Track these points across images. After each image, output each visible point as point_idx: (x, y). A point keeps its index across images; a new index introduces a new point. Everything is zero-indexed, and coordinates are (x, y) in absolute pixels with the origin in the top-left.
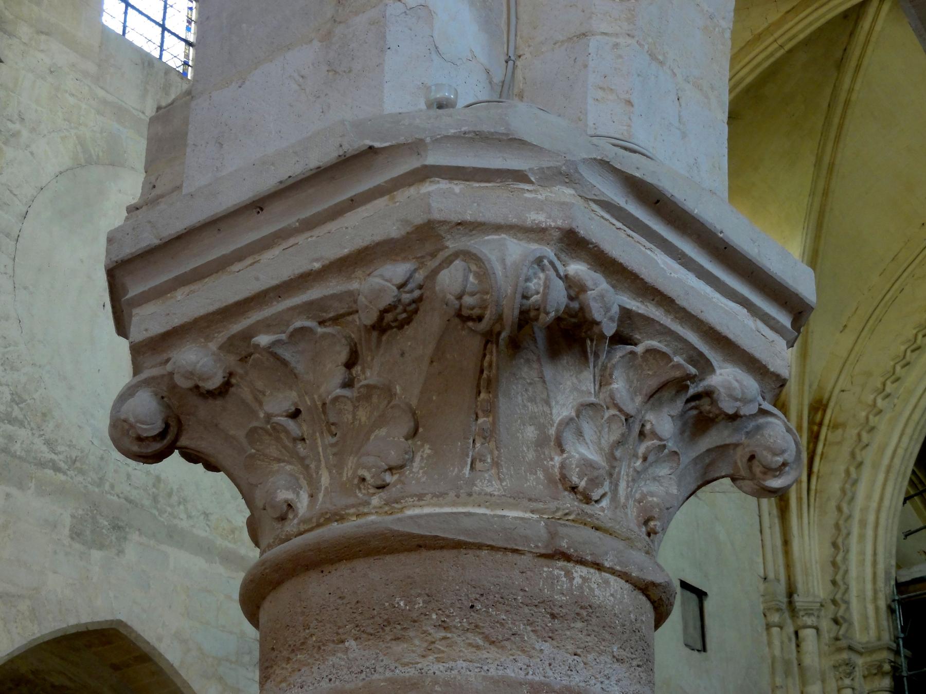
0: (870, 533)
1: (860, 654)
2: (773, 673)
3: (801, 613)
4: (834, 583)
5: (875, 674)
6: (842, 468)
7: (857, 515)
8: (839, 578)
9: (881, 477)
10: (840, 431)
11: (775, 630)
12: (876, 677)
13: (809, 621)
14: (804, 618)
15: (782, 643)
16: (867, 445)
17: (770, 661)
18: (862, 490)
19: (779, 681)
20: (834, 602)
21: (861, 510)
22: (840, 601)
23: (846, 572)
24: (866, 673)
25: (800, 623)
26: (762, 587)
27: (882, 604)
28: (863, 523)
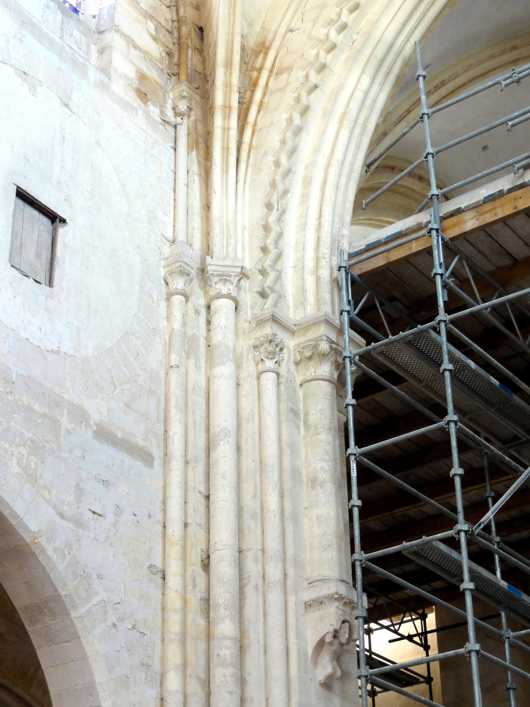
1: (292, 333)
2: (168, 352)
3: (215, 279)
4: (264, 250)
5: (310, 358)
6: (285, 116)
7: (300, 171)
8: (270, 242)
9: (333, 126)
10: (285, 76)
11: (177, 299)
12: (312, 363)
13: (224, 289)
14: (218, 286)
15: (185, 315)
16: (316, 87)
17: (167, 337)
19: (174, 359)
20: (263, 272)
21: (307, 167)
23: (280, 235)
24: (299, 358)
25: (212, 292)
26: (167, 250)
27: (325, 273)
28: (307, 182)
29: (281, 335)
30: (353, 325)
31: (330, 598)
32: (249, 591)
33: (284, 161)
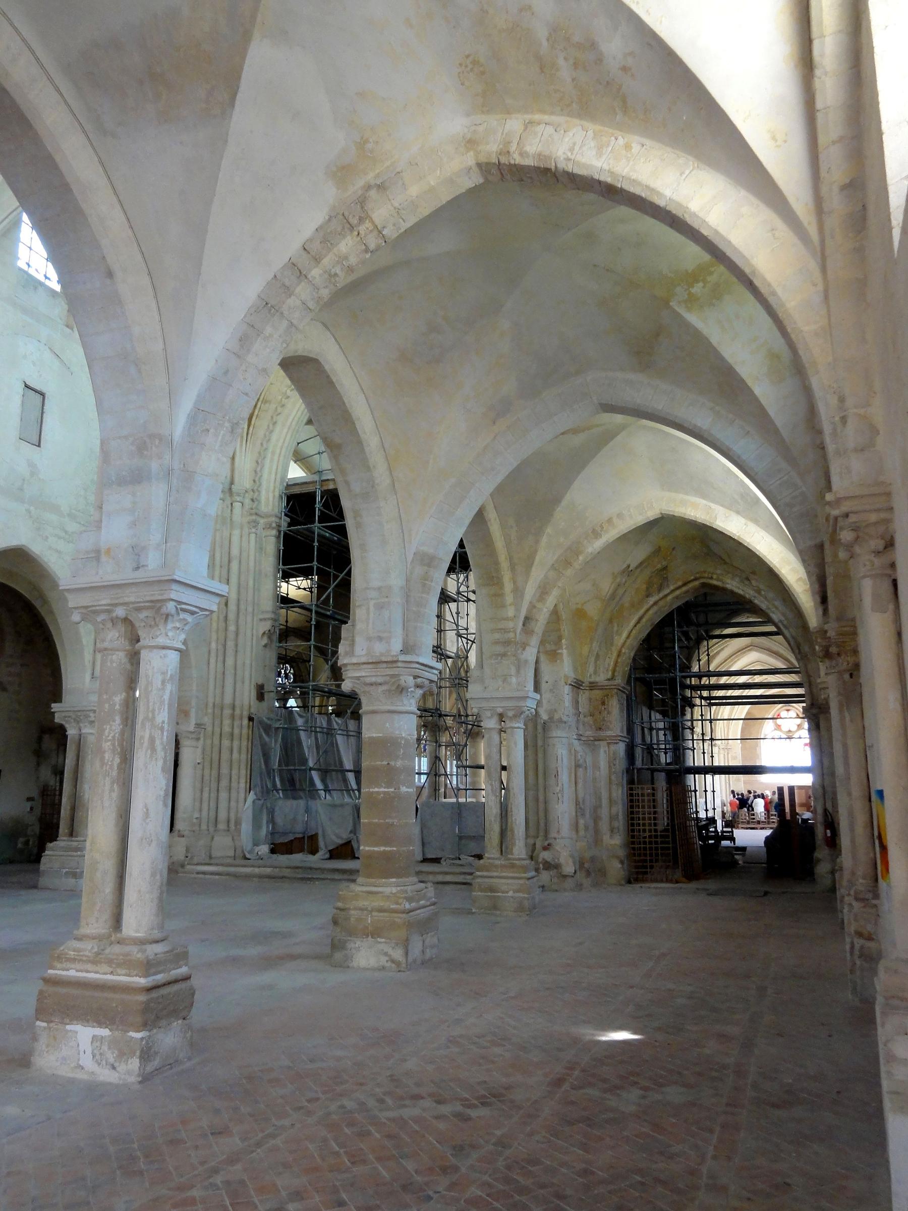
0: (276, 458)
1: (261, 517)
3: (235, 494)
4: (254, 481)
8: (257, 479)
9: (285, 430)
10: (267, 405)
16: (280, 414)
18: (274, 437)
20: (253, 491)
22: (256, 491)
23: (261, 476)
27: (277, 494)
28: (273, 453)
29: (259, 519)
30: (286, 515)
31: (269, 619)
32: (241, 614)
33: (265, 446)
